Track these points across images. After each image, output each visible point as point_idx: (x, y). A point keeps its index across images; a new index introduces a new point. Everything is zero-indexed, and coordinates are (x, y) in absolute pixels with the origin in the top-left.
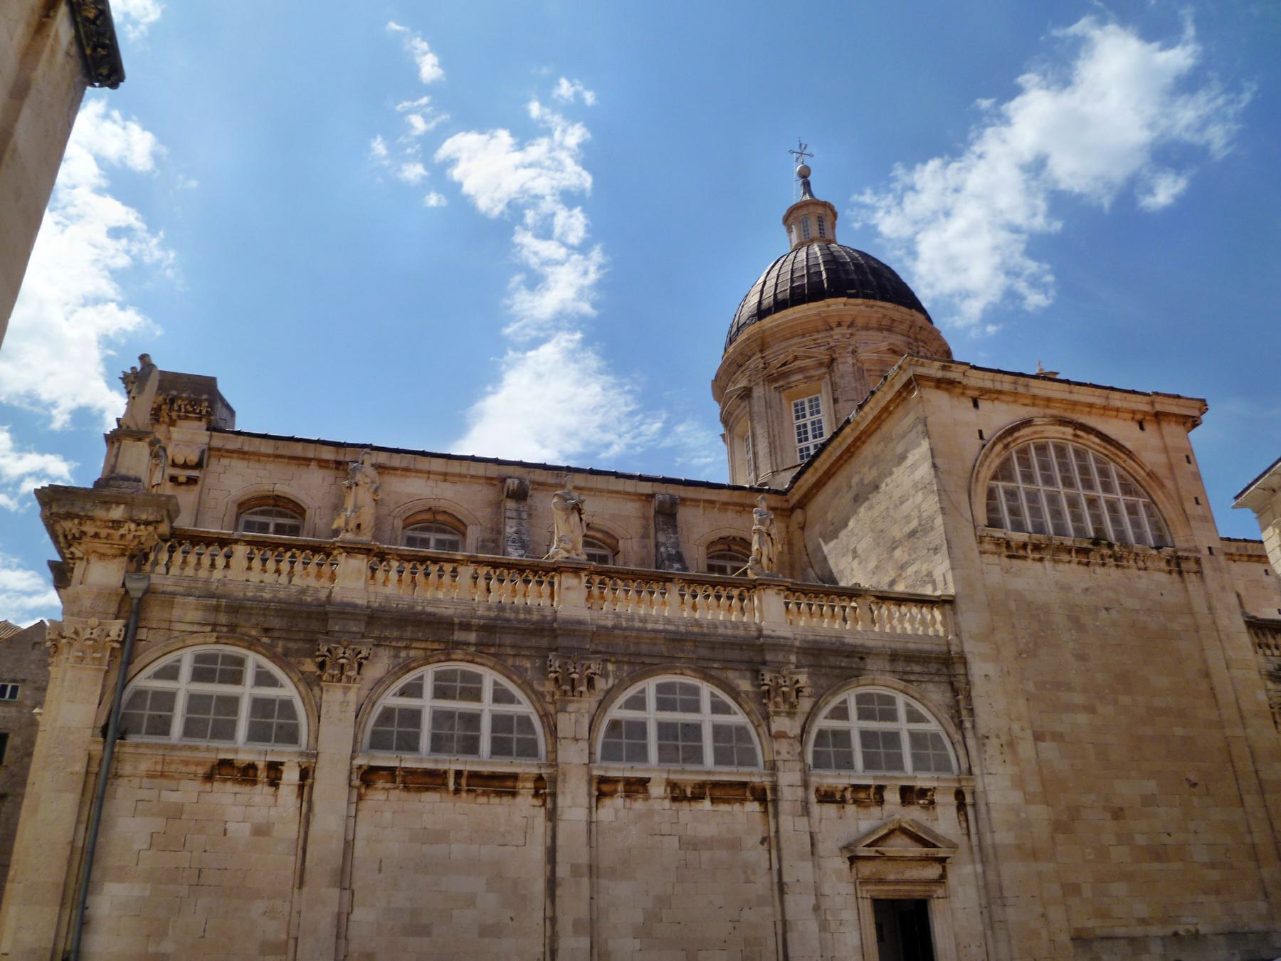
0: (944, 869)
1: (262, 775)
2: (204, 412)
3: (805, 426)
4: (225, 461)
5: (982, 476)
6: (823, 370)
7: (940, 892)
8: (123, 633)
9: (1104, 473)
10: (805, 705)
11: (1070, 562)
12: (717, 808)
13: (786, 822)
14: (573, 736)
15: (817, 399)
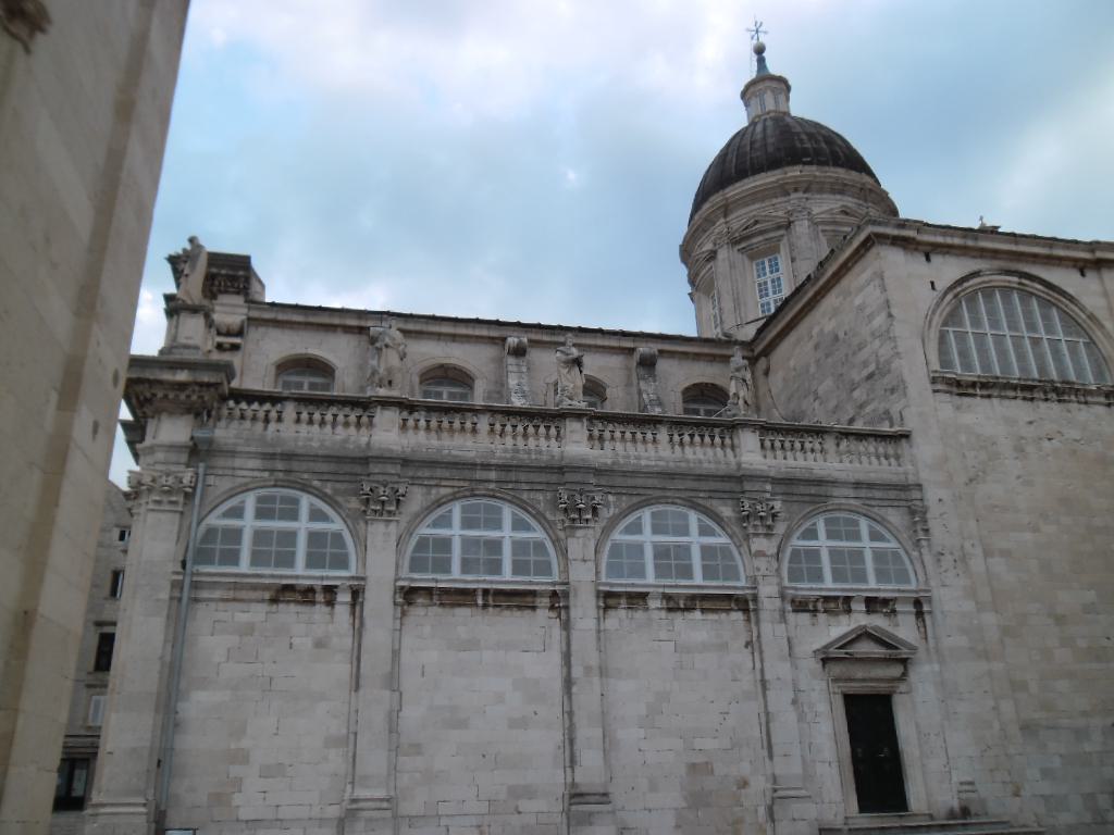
0: (906, 668)
1: (320, 597)
2: (241, 286)
3: (766, 283)
4: (262, 330)
5: (934, 323)
6: (782, 232)
7: (903, 687)
8: (194, 480)
9: (1046, 318)
10: (780, 528)
11: (1015, 398)
12: (704, 617)
13: (767, 628)
14: (581, 557)
15: (776, 259)
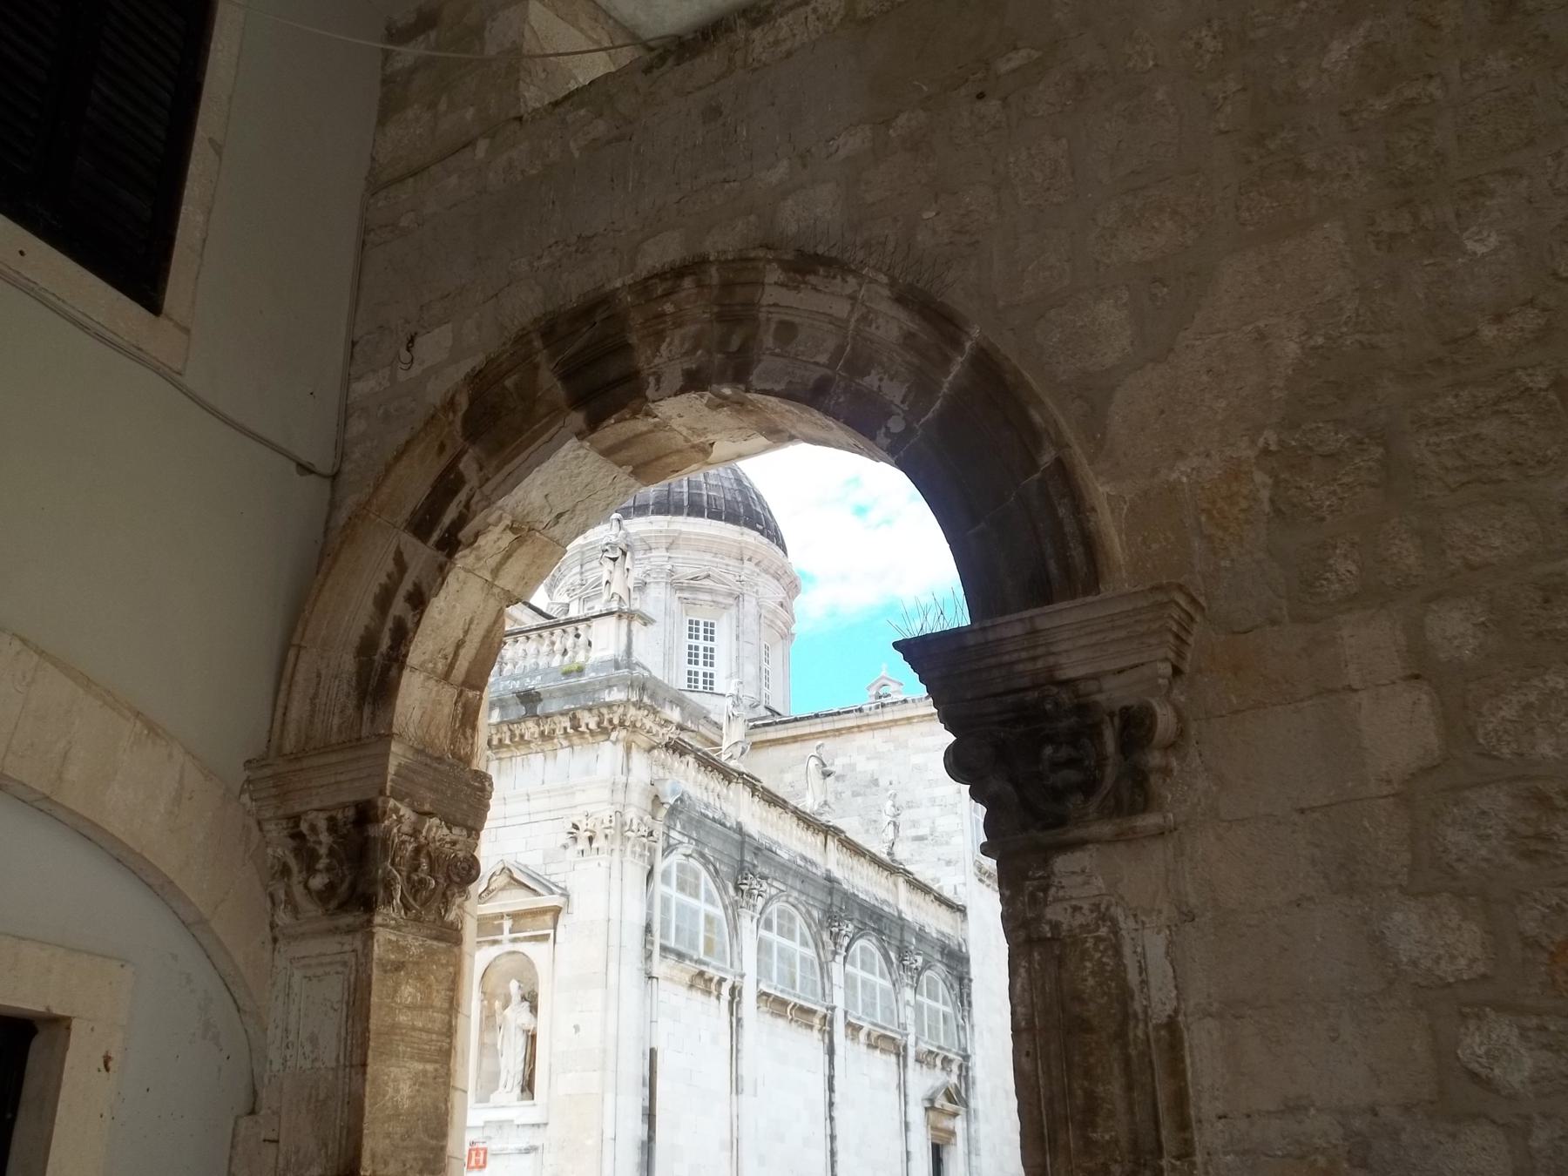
6: (731, 601)
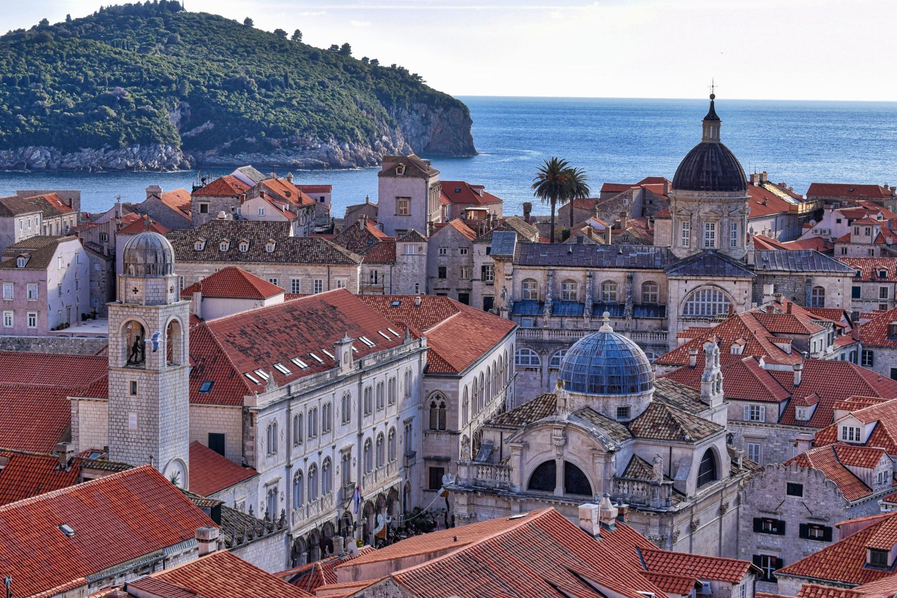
9: (720, 296)
